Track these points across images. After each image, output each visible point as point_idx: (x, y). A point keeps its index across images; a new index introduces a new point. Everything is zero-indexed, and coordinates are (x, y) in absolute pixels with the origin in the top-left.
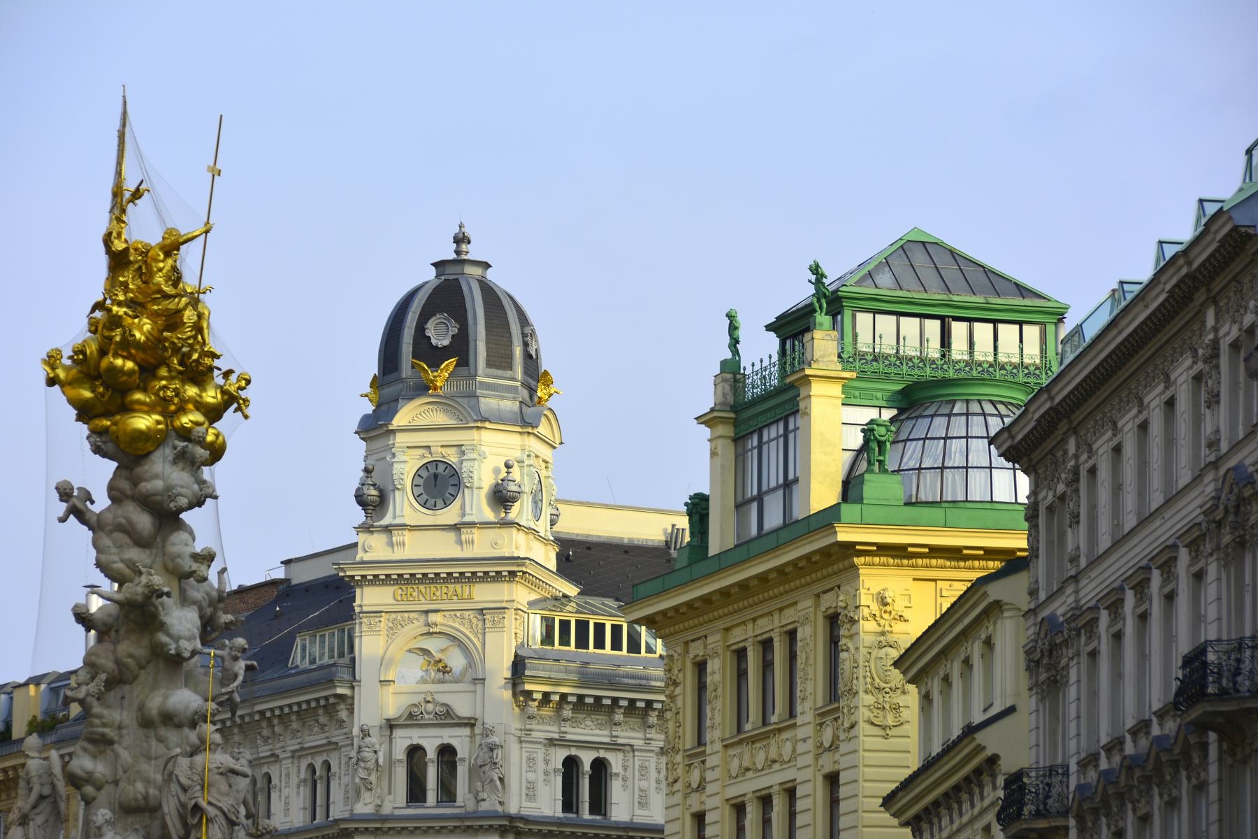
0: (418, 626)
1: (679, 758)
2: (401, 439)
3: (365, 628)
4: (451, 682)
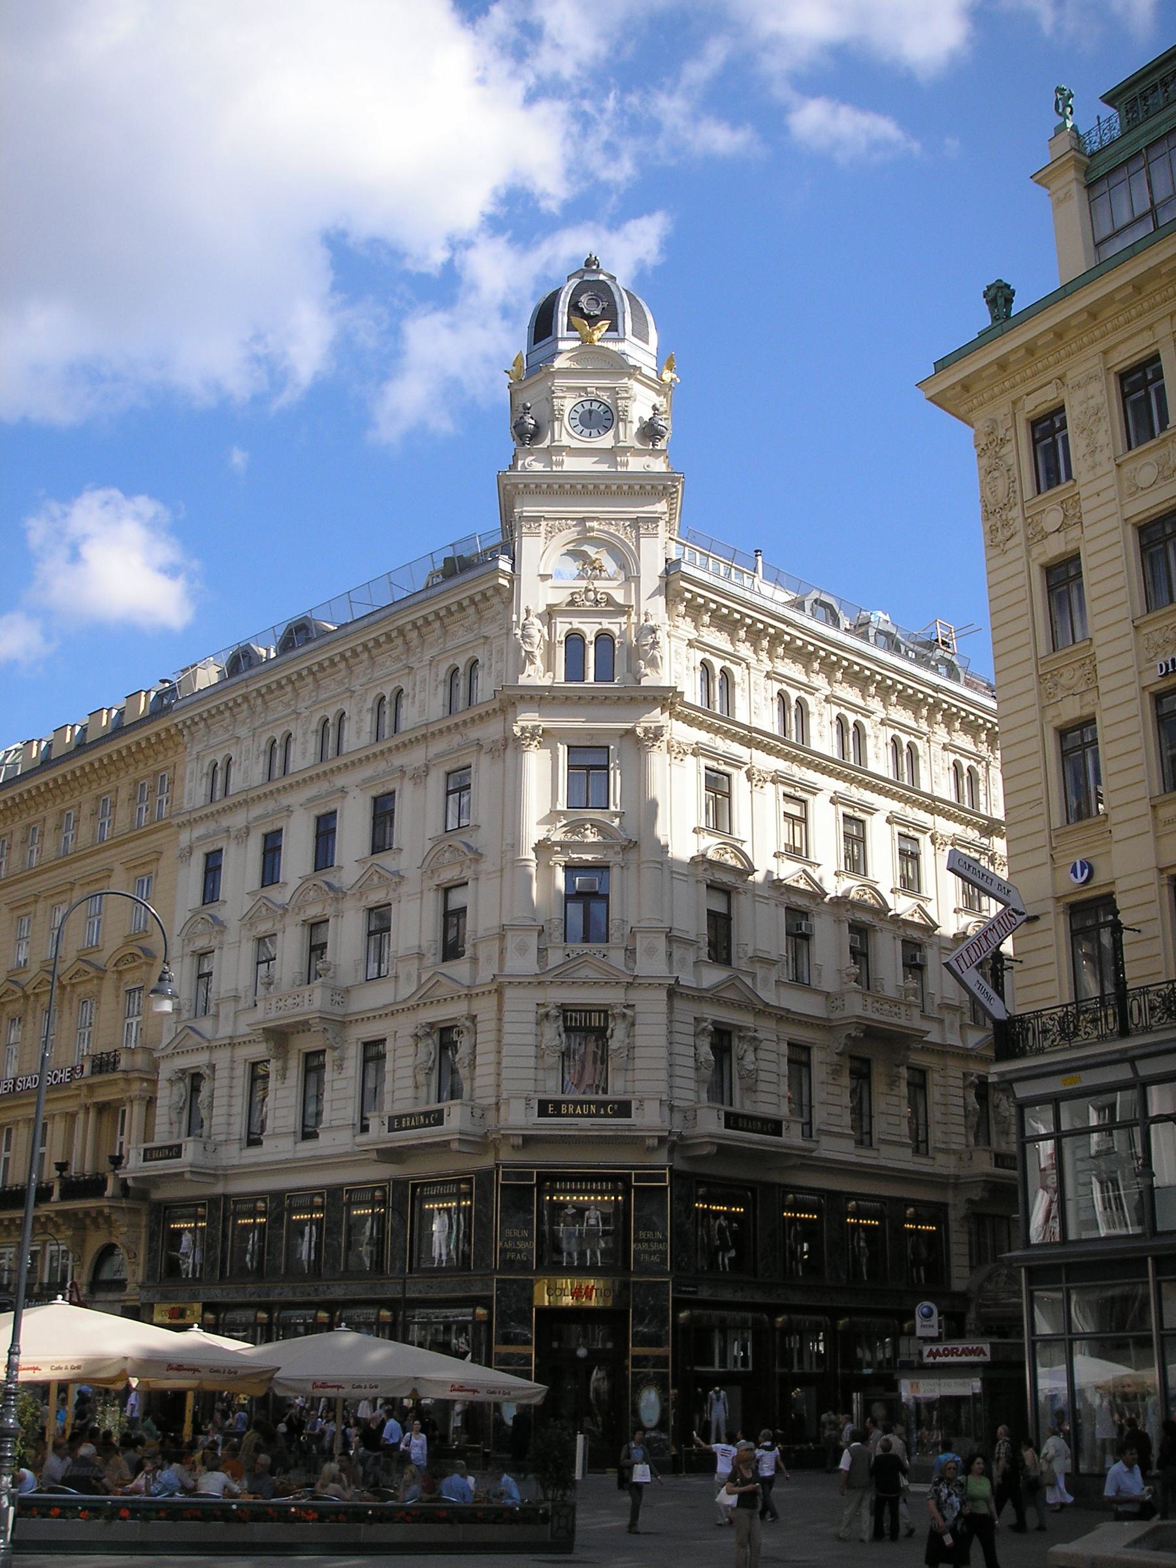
0: (571, 533)
1: (1016, 512)
2: (558, 382)
3: (524, 530)
4: (606, 579)
